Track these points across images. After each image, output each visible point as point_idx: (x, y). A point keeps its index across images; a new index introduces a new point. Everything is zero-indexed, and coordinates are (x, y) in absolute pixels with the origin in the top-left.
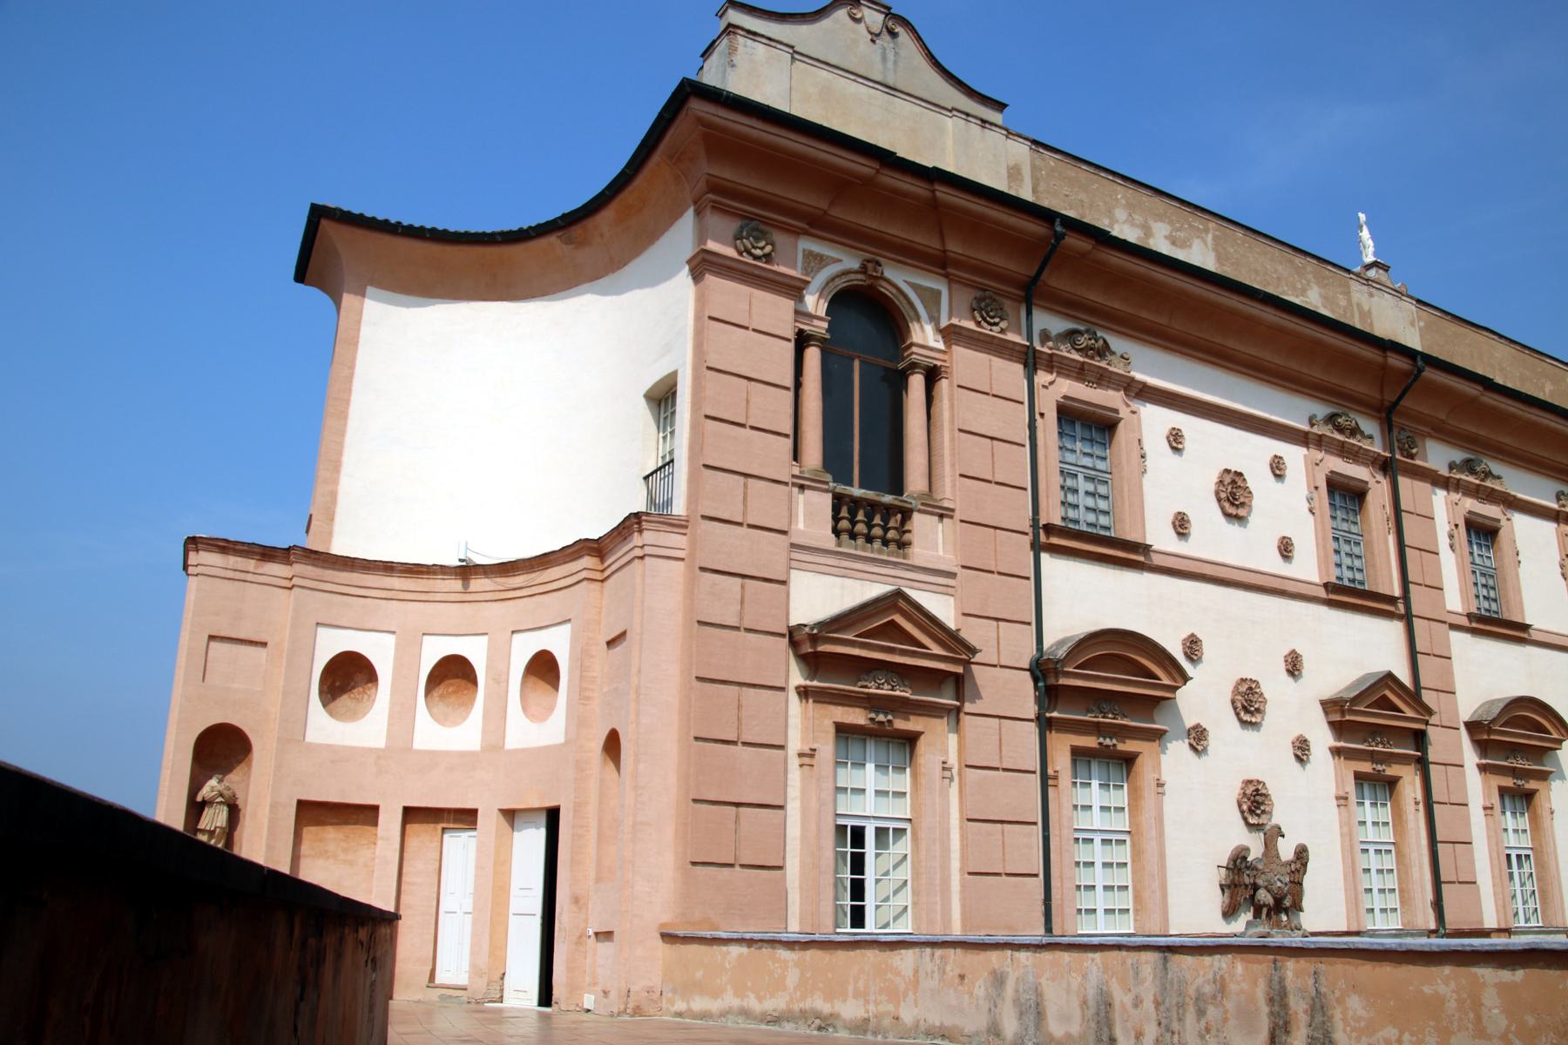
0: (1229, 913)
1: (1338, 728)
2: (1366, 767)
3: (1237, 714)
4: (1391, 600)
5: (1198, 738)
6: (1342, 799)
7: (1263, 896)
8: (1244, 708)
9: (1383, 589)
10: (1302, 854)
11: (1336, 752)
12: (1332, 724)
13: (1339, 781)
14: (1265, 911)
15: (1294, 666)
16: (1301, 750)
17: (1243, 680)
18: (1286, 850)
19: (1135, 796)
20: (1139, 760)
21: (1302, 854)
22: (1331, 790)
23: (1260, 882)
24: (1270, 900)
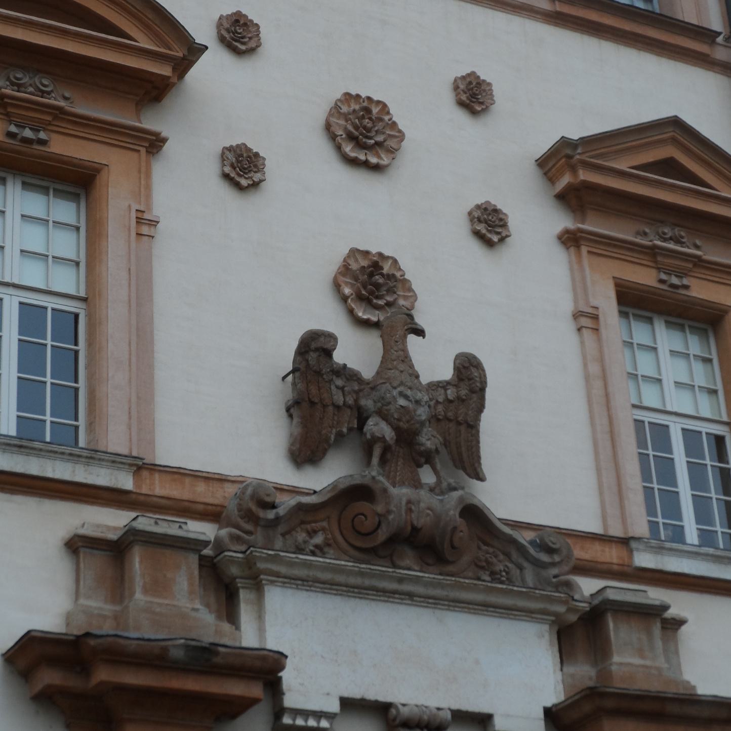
0: (305, 453)
1: (573, 199)
2: (644, 277)
3: (339, 148)
4: (706, 35)
5: (242, 169)
6: (586, 319)
7: (378, 427)
8: (351, 137)
9: (689, 16)
10: (469, 371)
11: (570, 240)
12: (562, 197)
13: (579, 287)
14: (377, 451)
15: (473, 96)
16: (489, 226)
17: (348, 97)
18: (432, 362)
19: (94, 234)
20: (102, 177)
21: (469, 371)
22: (567, 306)
23: (367, 403)
24: (388, 433)
